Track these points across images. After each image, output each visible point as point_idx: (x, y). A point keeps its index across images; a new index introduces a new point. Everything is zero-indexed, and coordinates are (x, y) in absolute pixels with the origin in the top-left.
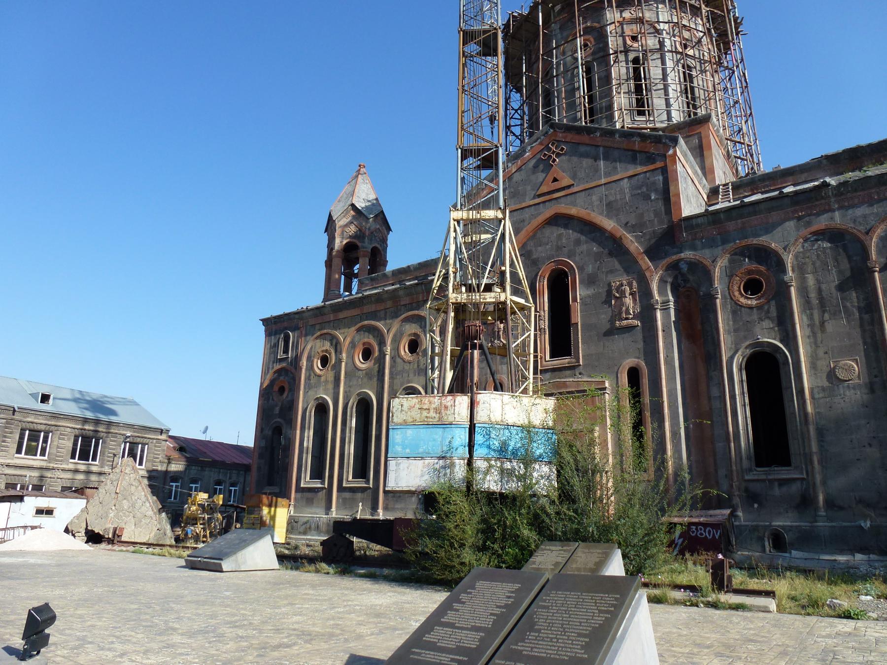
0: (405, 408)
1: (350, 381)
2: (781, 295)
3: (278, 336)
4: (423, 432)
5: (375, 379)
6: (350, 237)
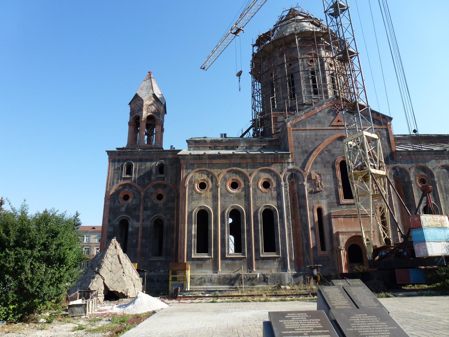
0: (427, 220)
1: (225, 198)
3: (121, 163)
4: (437, 231)
5: (243, 199)
6: (152, 112)
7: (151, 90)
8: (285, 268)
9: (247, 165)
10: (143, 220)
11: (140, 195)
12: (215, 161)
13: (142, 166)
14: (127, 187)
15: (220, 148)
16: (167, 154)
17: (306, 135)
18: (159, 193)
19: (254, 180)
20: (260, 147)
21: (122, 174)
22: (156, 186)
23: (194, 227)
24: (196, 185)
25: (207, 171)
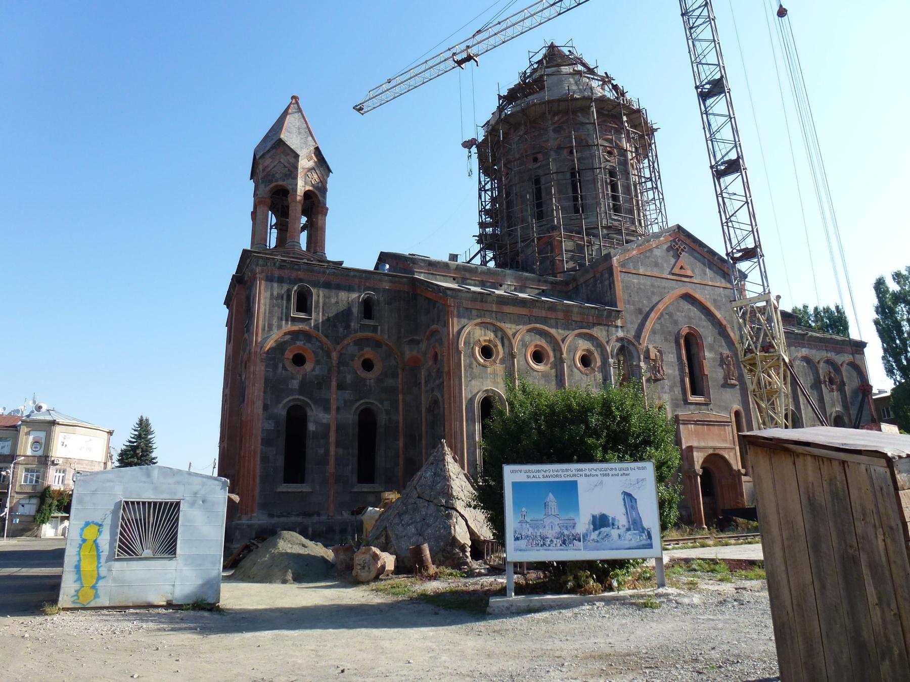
7: (310, 138)
9: (557, 323)
10: (338, 409)
11: (328, 355)
13: (329, 297)
14: (301, 337)
15: (473, 282)
16: (380, 280)
17: (639, 283)
18: (367, 356)
19: (569, 351)
20: (537, 291)
21: (288, 308)
22: (360, 343)
24: (477, 349)
25: (494, 325)
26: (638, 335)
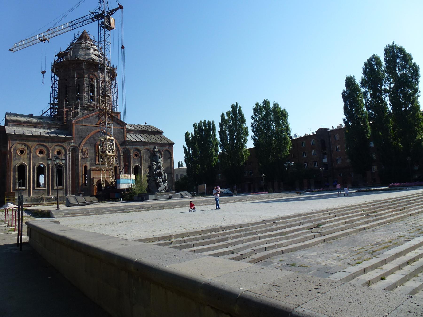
2: (140, 157)
8: (66, 194)
12: (30, 139)
19: (52, 150)
23: (17, 174)
26: (79, 145)
